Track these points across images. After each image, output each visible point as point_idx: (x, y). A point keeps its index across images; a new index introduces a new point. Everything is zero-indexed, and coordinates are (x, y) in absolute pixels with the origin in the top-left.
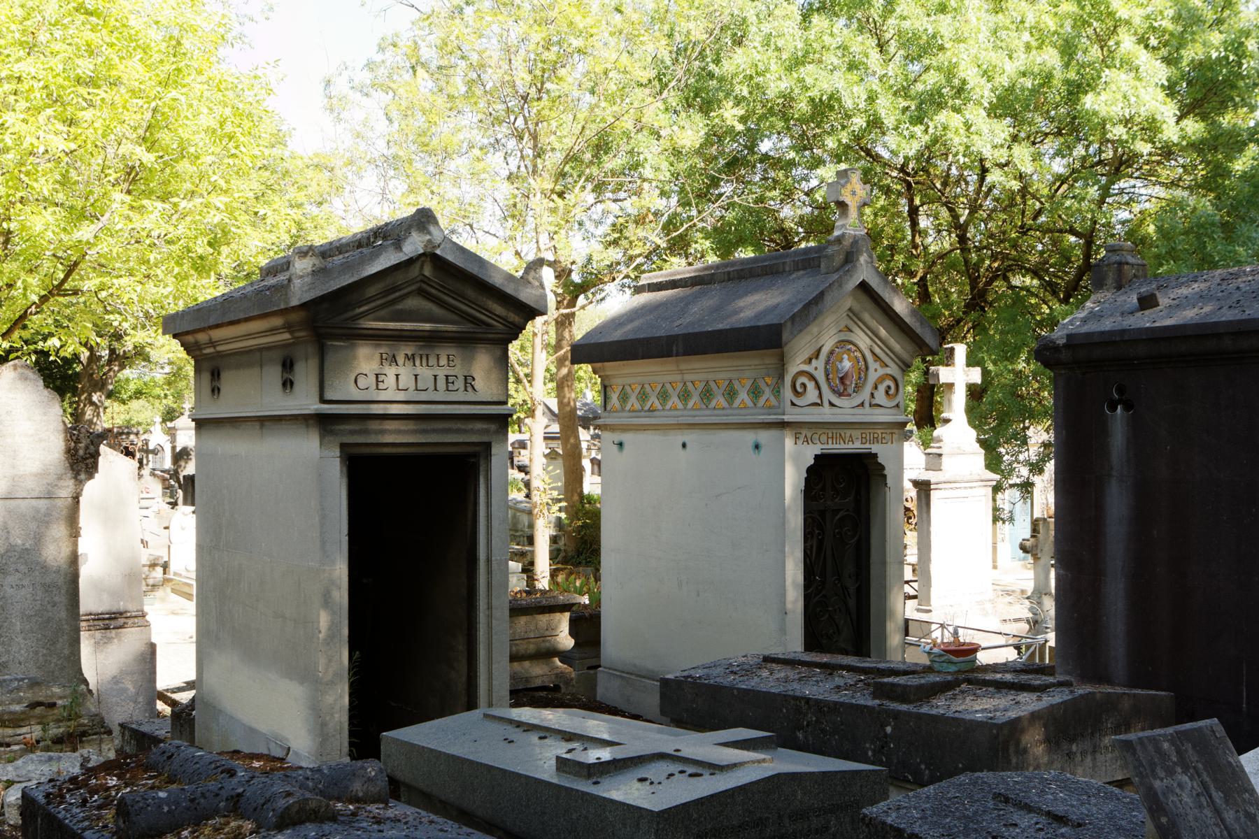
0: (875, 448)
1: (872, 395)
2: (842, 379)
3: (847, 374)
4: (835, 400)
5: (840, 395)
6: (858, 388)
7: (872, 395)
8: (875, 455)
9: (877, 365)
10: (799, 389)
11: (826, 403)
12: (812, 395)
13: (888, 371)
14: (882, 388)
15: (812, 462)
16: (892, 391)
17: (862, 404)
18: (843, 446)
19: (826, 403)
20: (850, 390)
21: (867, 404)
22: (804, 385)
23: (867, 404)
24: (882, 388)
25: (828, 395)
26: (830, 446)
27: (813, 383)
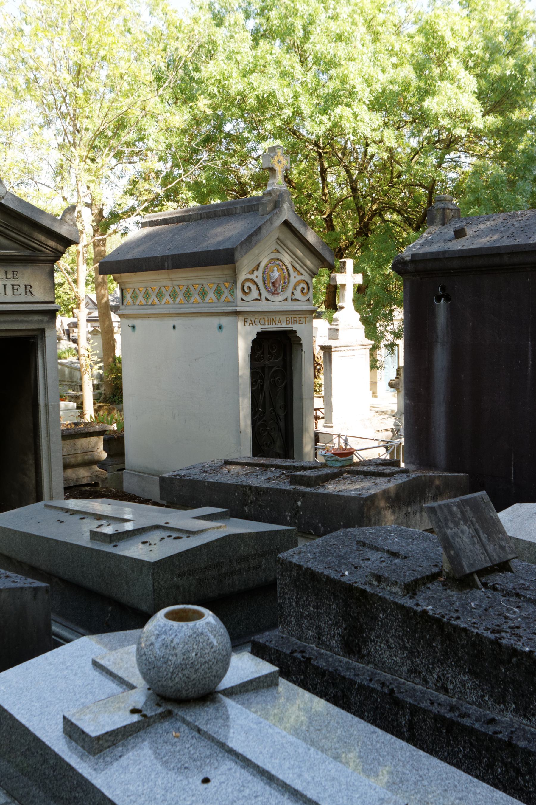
0: (295, 327)
2: (273, 283)
3: (276, 280)
4: (269, 297)
5: (273, 293)
6: (283, 289)
8: (295, 332)
9: (296, 274)
12: (255, 294)
13: (302, 277)
14: (299, 289)
15: (255, 336)
16: (305, 291)
17: (287, 299)
18: (274, 326)
21: (289, 299)
22: (249, 288)
23: (289, 299)
24: (299, 289)
25: (265, 294)
26: (266, 326)
27: (255, 286)
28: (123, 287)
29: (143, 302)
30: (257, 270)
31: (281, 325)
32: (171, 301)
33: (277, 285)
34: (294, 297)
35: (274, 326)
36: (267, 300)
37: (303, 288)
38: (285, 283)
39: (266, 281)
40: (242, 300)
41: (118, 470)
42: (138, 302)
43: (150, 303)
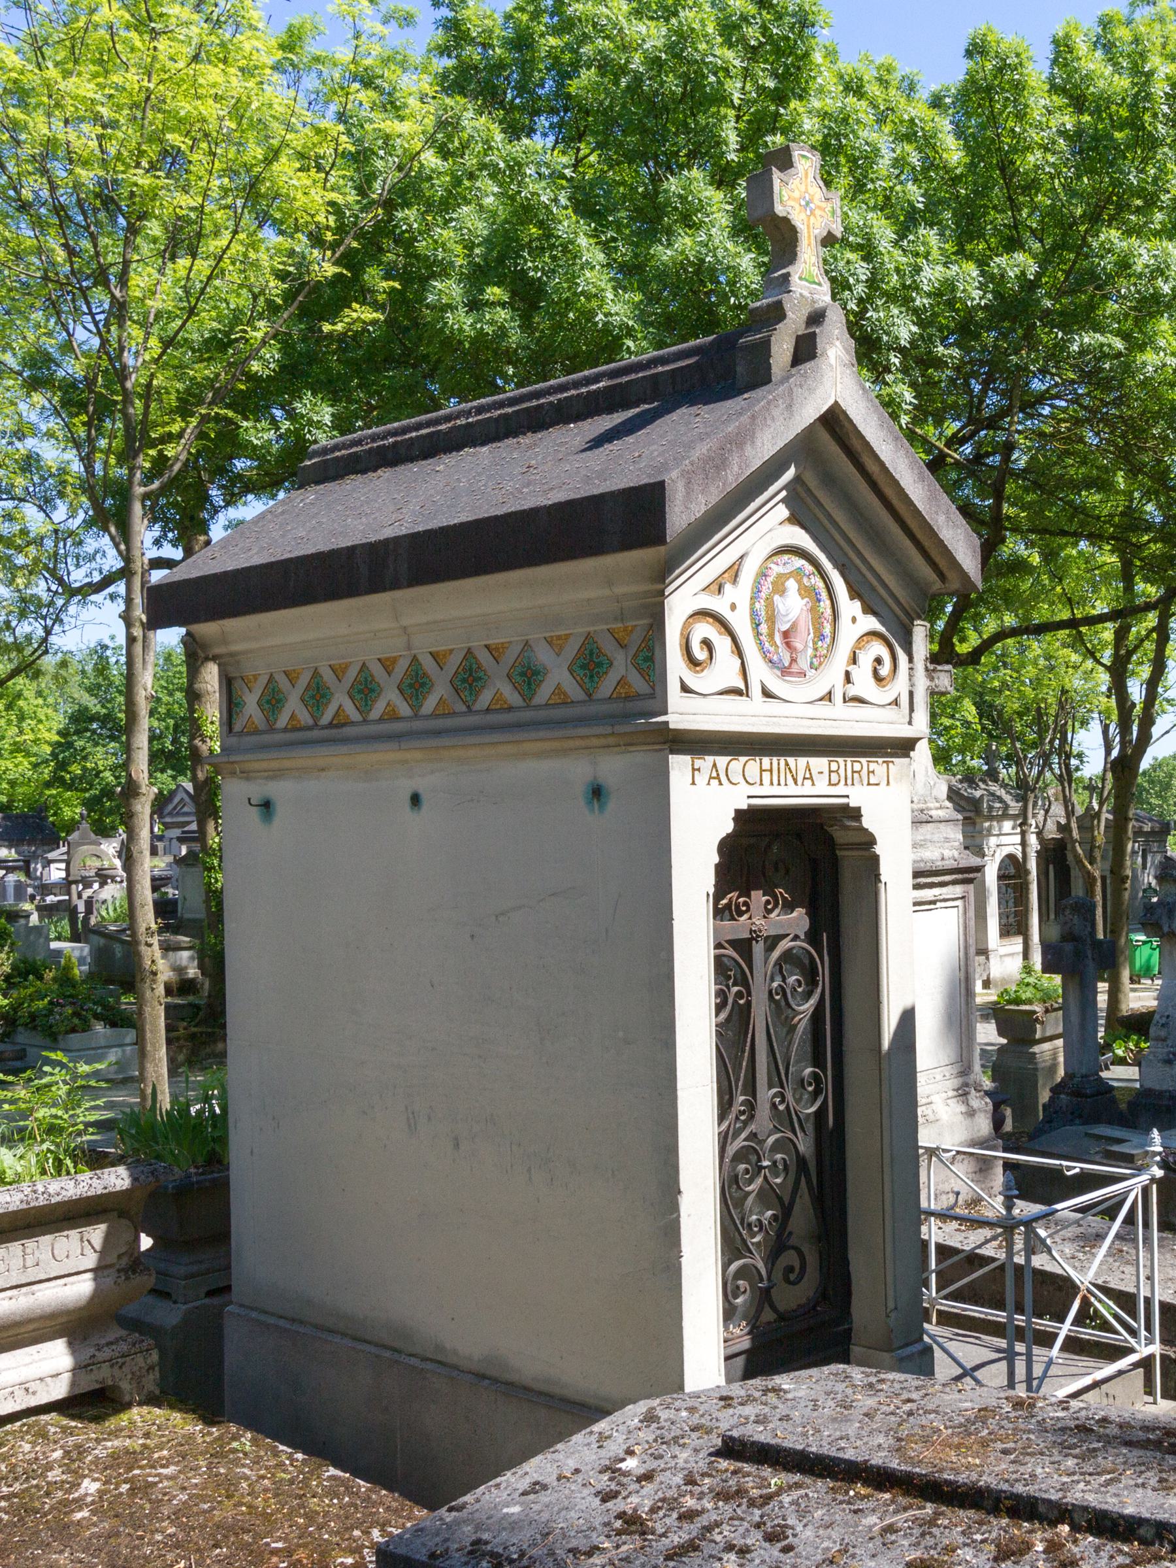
0: (857, 796)
1: (848, 678)
3: (794, 626)
6: (819, 661)
7: (848, 678)
10: (700, 654)
11: (756, 690)
14: (866, 659)
16: (885, 671)
17: (828, 697)
19: (756, 690)
20: (803, 663)
22: (707, 644)
23: (838, 697)
24: (866, 659)
26: (766, 790)
27: (729, 640)
28: (233, 673)
29: (305, 718)
30: (735, 580)
31: (809, 784)
32: (404, 709)
33: (798, 645)
34: (853, 691)
35: (791, 789)
36: (767, 694)
37: (878, 661)
38: (822, 637)
39: (764, 629)
40: (685, 689)
41: (210, 1294)
42: (283, 721)
43: (326, 719)
